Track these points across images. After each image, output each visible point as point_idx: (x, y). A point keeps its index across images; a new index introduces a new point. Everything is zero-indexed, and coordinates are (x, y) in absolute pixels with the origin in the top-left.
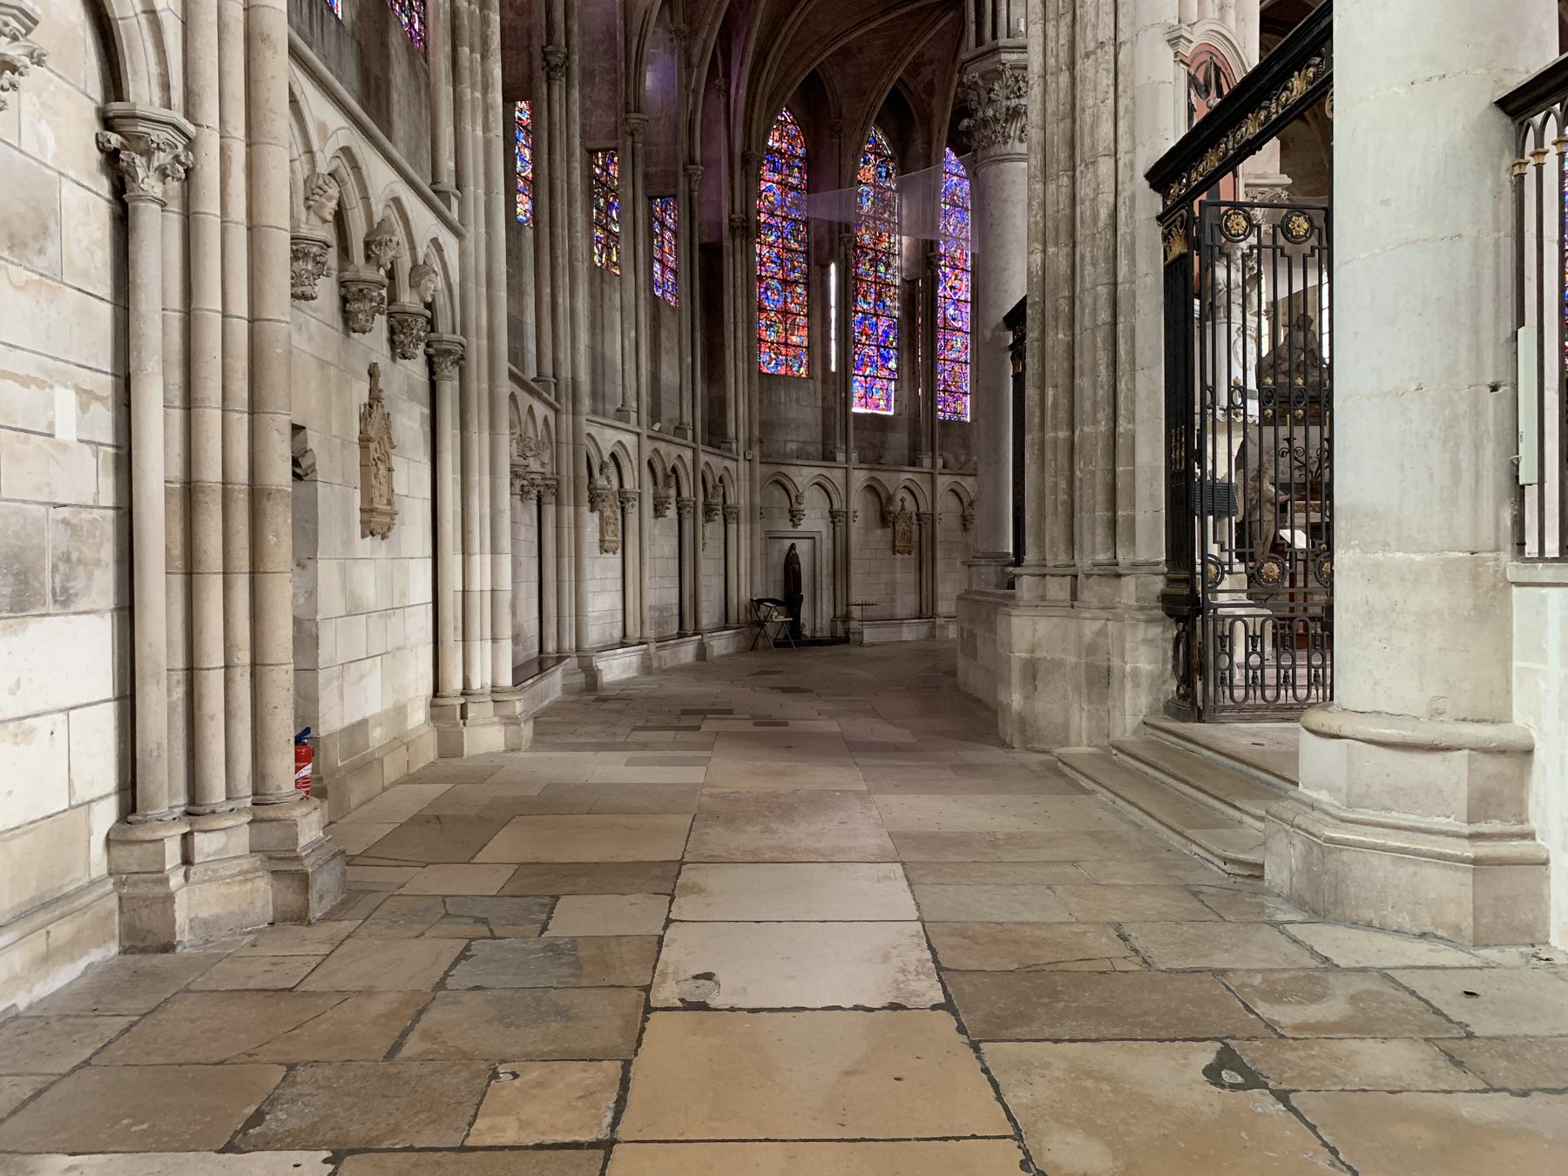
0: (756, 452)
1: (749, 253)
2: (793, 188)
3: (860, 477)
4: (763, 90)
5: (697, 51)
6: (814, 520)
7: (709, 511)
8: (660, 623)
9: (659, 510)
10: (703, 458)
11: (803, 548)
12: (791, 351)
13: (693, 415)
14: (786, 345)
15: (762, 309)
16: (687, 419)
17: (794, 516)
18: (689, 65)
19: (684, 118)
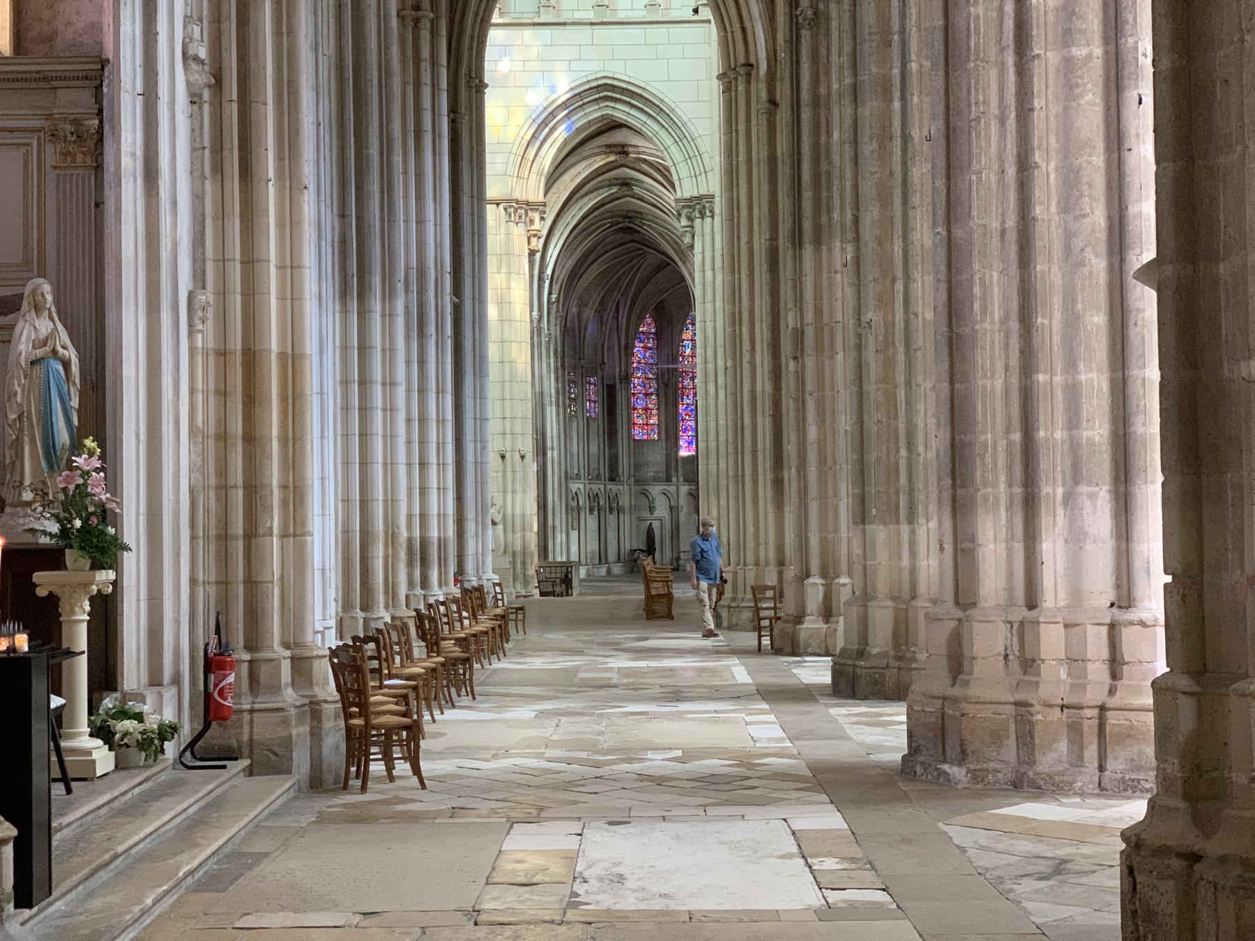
0: (632, 480)
1: (628, 389)
2: (650, 349)
3: (684, 489)
4: (634, 317)
5: (605, 318)
6: (662, 511)
7: (611, 510)
8: (591, 559)
9: (591, 511)
10: (609, 487)
11: (656, 525)
12: (650, 427)
13: (604, 470)
14: (647, 425)
15: (635, 409)
16: (602, 471)
17: (651, 509)
18: (602, 322)
19: (600, 345)
